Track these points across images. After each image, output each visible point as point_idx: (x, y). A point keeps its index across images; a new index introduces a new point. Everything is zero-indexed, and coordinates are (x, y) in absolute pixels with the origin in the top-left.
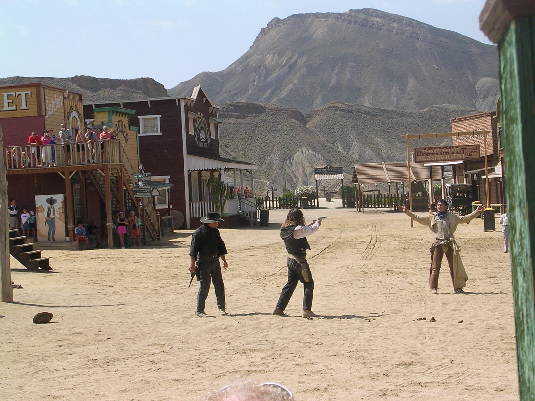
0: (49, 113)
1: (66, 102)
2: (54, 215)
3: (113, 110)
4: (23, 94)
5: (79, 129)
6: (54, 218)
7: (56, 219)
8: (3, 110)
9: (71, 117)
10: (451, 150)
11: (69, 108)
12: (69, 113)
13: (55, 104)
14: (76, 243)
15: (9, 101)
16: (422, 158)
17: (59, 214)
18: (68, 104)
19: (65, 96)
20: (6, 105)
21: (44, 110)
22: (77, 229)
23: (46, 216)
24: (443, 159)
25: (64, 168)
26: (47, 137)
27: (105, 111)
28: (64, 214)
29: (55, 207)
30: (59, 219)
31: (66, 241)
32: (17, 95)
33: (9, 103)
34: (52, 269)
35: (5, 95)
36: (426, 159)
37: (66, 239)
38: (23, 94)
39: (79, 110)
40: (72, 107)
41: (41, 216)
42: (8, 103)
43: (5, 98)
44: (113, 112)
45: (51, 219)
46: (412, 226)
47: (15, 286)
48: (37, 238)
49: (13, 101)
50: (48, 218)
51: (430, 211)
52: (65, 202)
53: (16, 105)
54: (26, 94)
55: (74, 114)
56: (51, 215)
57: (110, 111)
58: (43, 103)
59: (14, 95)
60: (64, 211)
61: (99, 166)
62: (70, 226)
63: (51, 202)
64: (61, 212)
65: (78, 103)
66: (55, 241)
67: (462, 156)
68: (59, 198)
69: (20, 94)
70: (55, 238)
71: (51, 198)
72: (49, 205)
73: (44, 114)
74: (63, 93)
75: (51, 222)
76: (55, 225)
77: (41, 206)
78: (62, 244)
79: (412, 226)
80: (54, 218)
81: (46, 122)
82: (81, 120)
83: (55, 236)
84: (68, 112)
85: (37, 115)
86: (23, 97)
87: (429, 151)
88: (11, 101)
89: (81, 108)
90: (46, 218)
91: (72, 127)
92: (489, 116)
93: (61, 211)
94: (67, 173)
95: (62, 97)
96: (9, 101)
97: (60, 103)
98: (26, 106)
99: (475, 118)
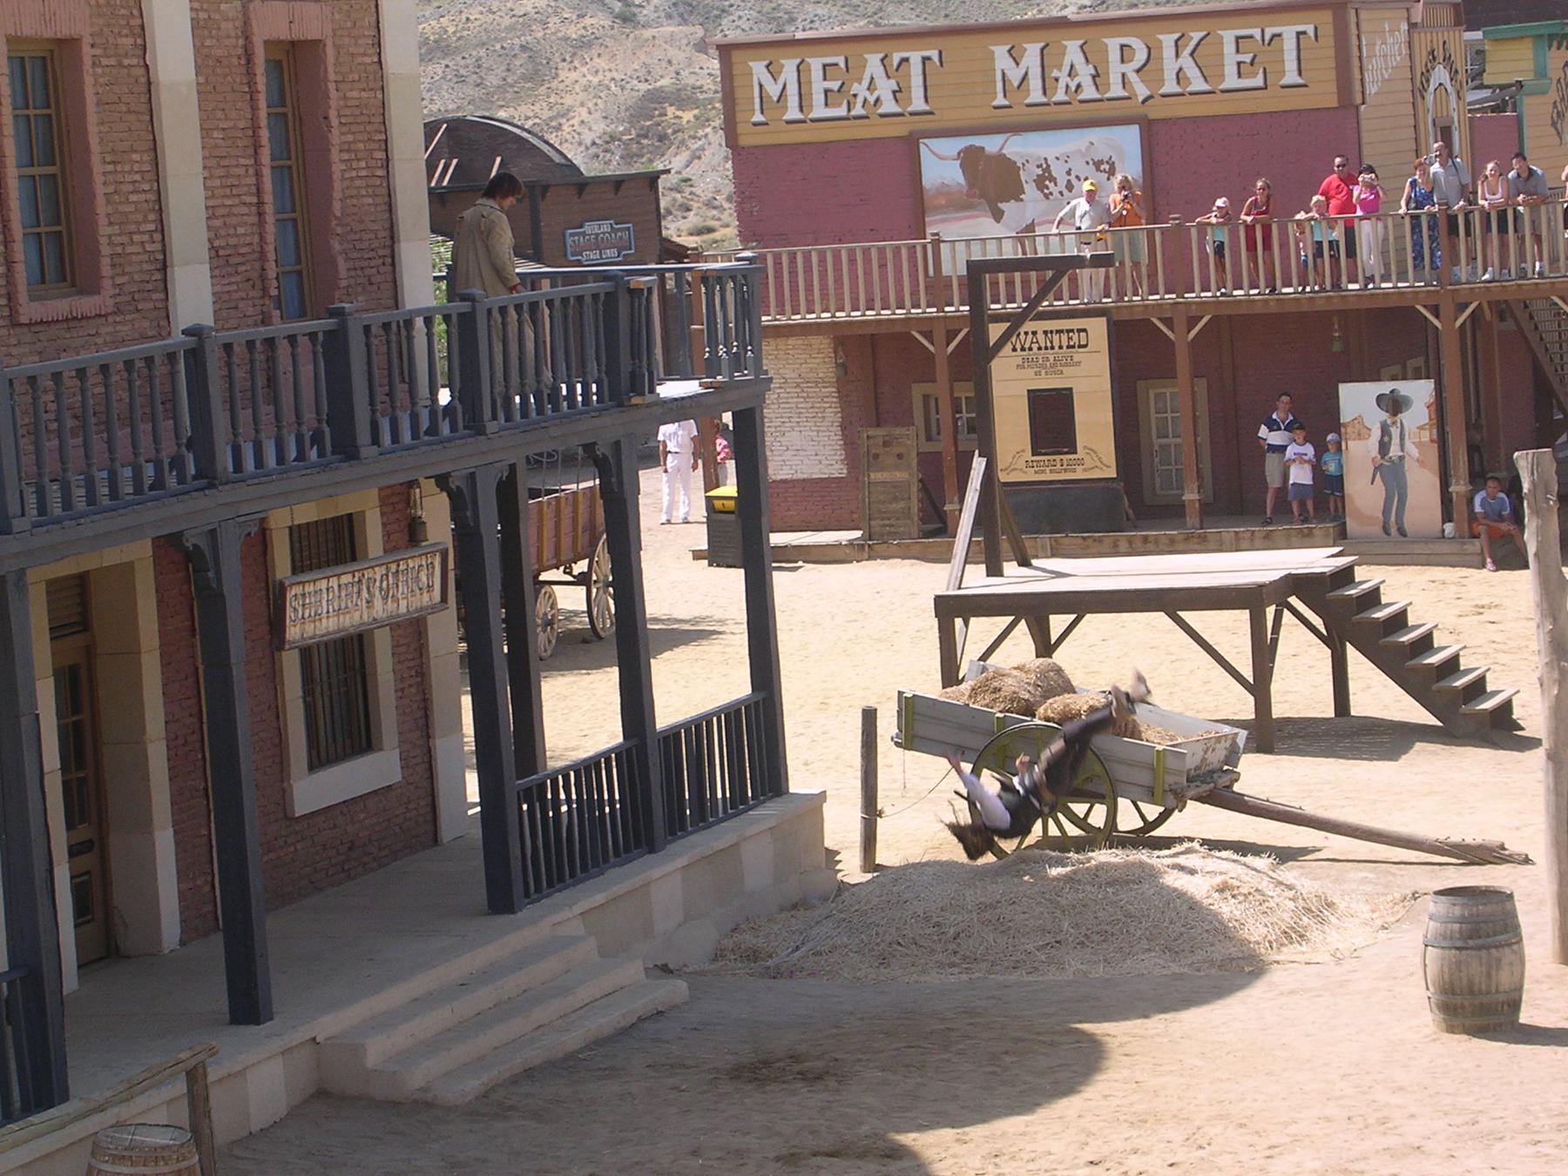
0: (1371, 89)
1: (1416, 36)
2: (1402, 450)
3: (1546, 32)
4: (1289, 33)
5: (1453, 122)
6: (1401, 458)
7: (1408, 464)
8: (1222, 87)
9: (1432, 88)
11: (1424, 54)
12: (1426, 76)
13: (1385, 56)
14: (1475, 546)
15: (1240, 58)
17: (1419, 445)
18: (1423, 42)
19: (1413, 21)
20: (1230, 70)
21: (1358, 87)
22: (1483, 501)
23: (1375, 452)
25: (1438, 292)
26: (1370, 187)
27: (1522, 38)
28: (1436, 445)
29: (1404, 421)
30: (1418, 460)
31: (1444, 537)
32: (1267, 38)
33: (1242, 65)
34: (1522, 729)
35: (1228, 36)
37: (1443, 531)
38: (1289, 33)
39: (1452, 58)
40: (1433, 51)
41: (1359, 455)
42: (1239, 64)
43: (1229, 48)
44: (1551, 37)
45: (1393, 462)
47: (1510, 856)
48: (1345, 523)
49: (1255, 56)
50: (1382, 458)
52: (1439, 407)
53: (1265, 69)
54: (1299, 34)
55: (1440, 74)
56: (1392, 449)
57: (1541, 36)
58: (1356, 62)
59: (1258, 37)
60: (1435, 437)
61: (1558, 286)
62: (1459, 488)
63: (1394, 405)
64: (1427, 439)
65: (1451, 33)
66: (1405, 536)
68: (1420, 392)
69: (1279, 35)
70: (1406, 526)
71: (1392, 392)
72: (1384, 416)
73: (1358, 99)
74: (1408, 10)
75: (1390, 472)
76: (1406, 484)
77: (1358, 420)
78: (1431, 546)
80: (1401, 458)
81: (1363, 123)
82: (1458, 93)
83: (1405, 520)
84: (1423, 73)
85: (1336, 105)
86: (1289, 44)
88: (1247, 58)
89: (1458, 56)
90: (1373, 459)
91: (1434, 120)
93: (1426, 436)
94: (1447, 309)
95: (1404, 27)
96: (1240, 58)
97: (1400, 47)
98: (1300, 74)
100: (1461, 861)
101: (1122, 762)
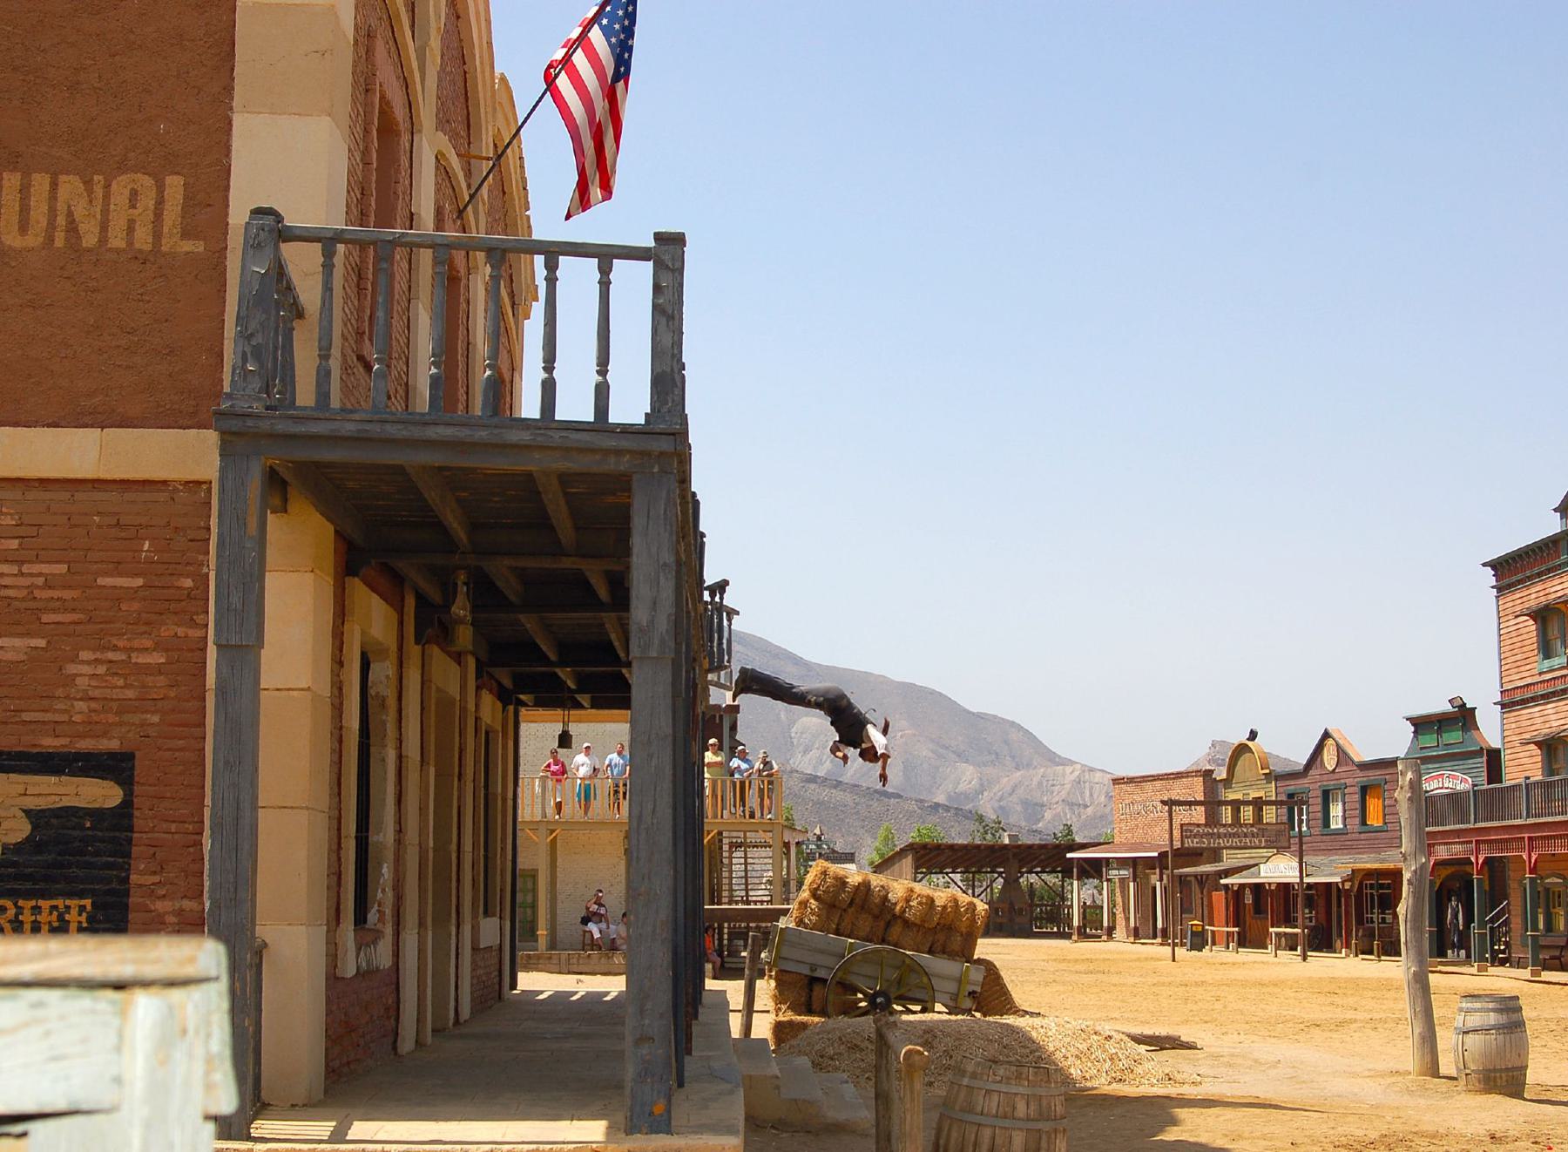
10: (1243, 831)
16: (1193, 843)
24: (1228, 845)
36: (1199, 845)
46: (1174, 960)
51: (1075, 937)
67: (1260, 841)
79: (1174, 960)
87: (1206, 831)
92: (1200, 776)
99: (1167, 779)
100: (1153, 1048)
101: (938, 976)
